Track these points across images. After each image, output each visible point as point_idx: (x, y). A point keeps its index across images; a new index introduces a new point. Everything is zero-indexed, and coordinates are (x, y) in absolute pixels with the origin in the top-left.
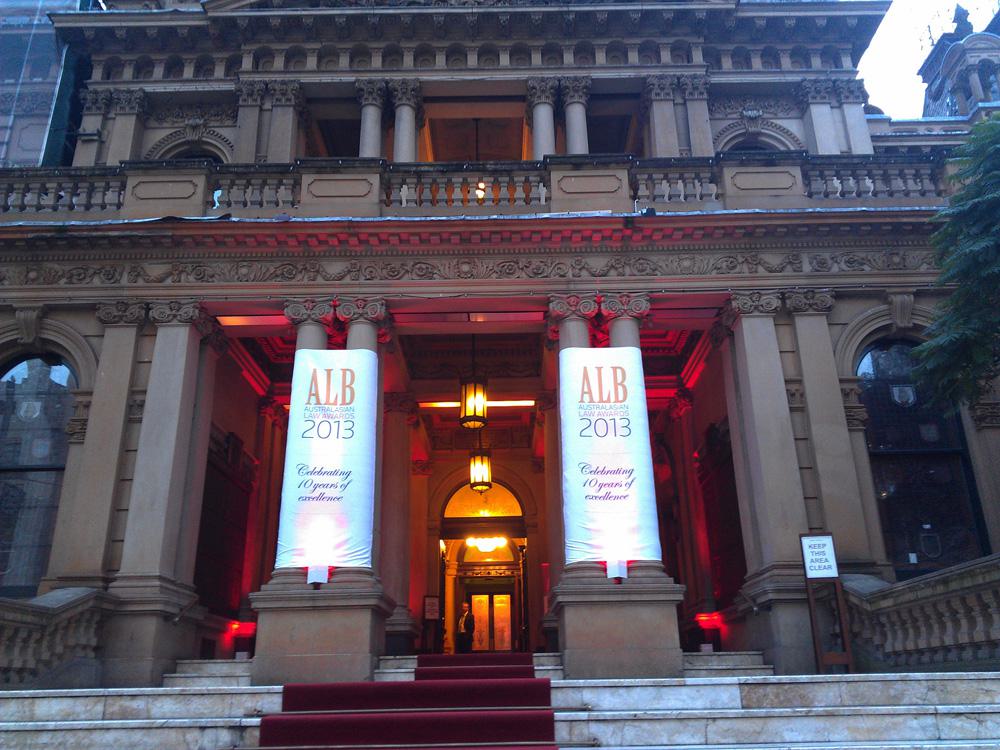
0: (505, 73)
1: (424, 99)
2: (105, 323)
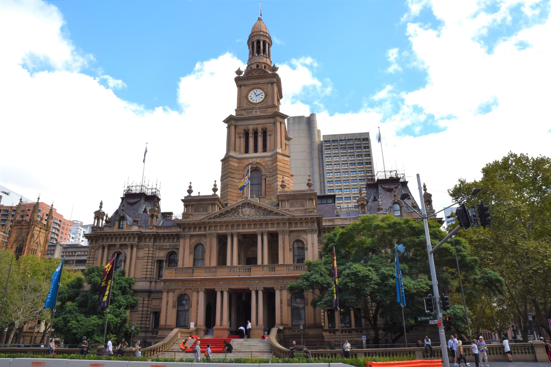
0: (252, 230)
1: (239, 234)
2: (193, 292)
